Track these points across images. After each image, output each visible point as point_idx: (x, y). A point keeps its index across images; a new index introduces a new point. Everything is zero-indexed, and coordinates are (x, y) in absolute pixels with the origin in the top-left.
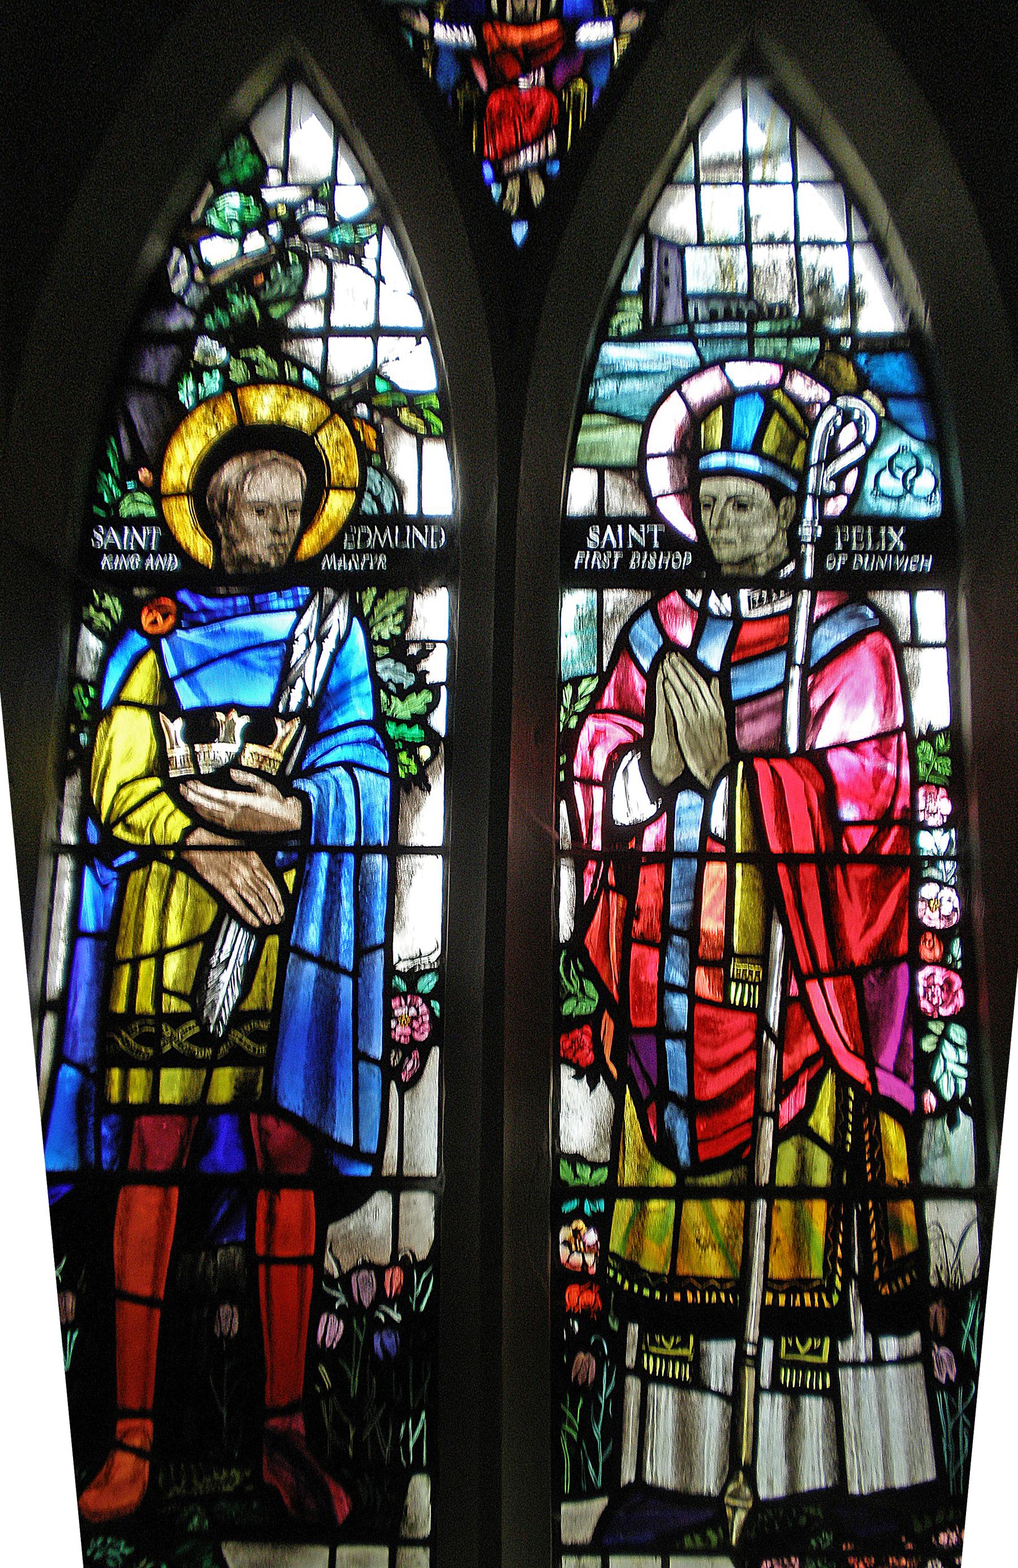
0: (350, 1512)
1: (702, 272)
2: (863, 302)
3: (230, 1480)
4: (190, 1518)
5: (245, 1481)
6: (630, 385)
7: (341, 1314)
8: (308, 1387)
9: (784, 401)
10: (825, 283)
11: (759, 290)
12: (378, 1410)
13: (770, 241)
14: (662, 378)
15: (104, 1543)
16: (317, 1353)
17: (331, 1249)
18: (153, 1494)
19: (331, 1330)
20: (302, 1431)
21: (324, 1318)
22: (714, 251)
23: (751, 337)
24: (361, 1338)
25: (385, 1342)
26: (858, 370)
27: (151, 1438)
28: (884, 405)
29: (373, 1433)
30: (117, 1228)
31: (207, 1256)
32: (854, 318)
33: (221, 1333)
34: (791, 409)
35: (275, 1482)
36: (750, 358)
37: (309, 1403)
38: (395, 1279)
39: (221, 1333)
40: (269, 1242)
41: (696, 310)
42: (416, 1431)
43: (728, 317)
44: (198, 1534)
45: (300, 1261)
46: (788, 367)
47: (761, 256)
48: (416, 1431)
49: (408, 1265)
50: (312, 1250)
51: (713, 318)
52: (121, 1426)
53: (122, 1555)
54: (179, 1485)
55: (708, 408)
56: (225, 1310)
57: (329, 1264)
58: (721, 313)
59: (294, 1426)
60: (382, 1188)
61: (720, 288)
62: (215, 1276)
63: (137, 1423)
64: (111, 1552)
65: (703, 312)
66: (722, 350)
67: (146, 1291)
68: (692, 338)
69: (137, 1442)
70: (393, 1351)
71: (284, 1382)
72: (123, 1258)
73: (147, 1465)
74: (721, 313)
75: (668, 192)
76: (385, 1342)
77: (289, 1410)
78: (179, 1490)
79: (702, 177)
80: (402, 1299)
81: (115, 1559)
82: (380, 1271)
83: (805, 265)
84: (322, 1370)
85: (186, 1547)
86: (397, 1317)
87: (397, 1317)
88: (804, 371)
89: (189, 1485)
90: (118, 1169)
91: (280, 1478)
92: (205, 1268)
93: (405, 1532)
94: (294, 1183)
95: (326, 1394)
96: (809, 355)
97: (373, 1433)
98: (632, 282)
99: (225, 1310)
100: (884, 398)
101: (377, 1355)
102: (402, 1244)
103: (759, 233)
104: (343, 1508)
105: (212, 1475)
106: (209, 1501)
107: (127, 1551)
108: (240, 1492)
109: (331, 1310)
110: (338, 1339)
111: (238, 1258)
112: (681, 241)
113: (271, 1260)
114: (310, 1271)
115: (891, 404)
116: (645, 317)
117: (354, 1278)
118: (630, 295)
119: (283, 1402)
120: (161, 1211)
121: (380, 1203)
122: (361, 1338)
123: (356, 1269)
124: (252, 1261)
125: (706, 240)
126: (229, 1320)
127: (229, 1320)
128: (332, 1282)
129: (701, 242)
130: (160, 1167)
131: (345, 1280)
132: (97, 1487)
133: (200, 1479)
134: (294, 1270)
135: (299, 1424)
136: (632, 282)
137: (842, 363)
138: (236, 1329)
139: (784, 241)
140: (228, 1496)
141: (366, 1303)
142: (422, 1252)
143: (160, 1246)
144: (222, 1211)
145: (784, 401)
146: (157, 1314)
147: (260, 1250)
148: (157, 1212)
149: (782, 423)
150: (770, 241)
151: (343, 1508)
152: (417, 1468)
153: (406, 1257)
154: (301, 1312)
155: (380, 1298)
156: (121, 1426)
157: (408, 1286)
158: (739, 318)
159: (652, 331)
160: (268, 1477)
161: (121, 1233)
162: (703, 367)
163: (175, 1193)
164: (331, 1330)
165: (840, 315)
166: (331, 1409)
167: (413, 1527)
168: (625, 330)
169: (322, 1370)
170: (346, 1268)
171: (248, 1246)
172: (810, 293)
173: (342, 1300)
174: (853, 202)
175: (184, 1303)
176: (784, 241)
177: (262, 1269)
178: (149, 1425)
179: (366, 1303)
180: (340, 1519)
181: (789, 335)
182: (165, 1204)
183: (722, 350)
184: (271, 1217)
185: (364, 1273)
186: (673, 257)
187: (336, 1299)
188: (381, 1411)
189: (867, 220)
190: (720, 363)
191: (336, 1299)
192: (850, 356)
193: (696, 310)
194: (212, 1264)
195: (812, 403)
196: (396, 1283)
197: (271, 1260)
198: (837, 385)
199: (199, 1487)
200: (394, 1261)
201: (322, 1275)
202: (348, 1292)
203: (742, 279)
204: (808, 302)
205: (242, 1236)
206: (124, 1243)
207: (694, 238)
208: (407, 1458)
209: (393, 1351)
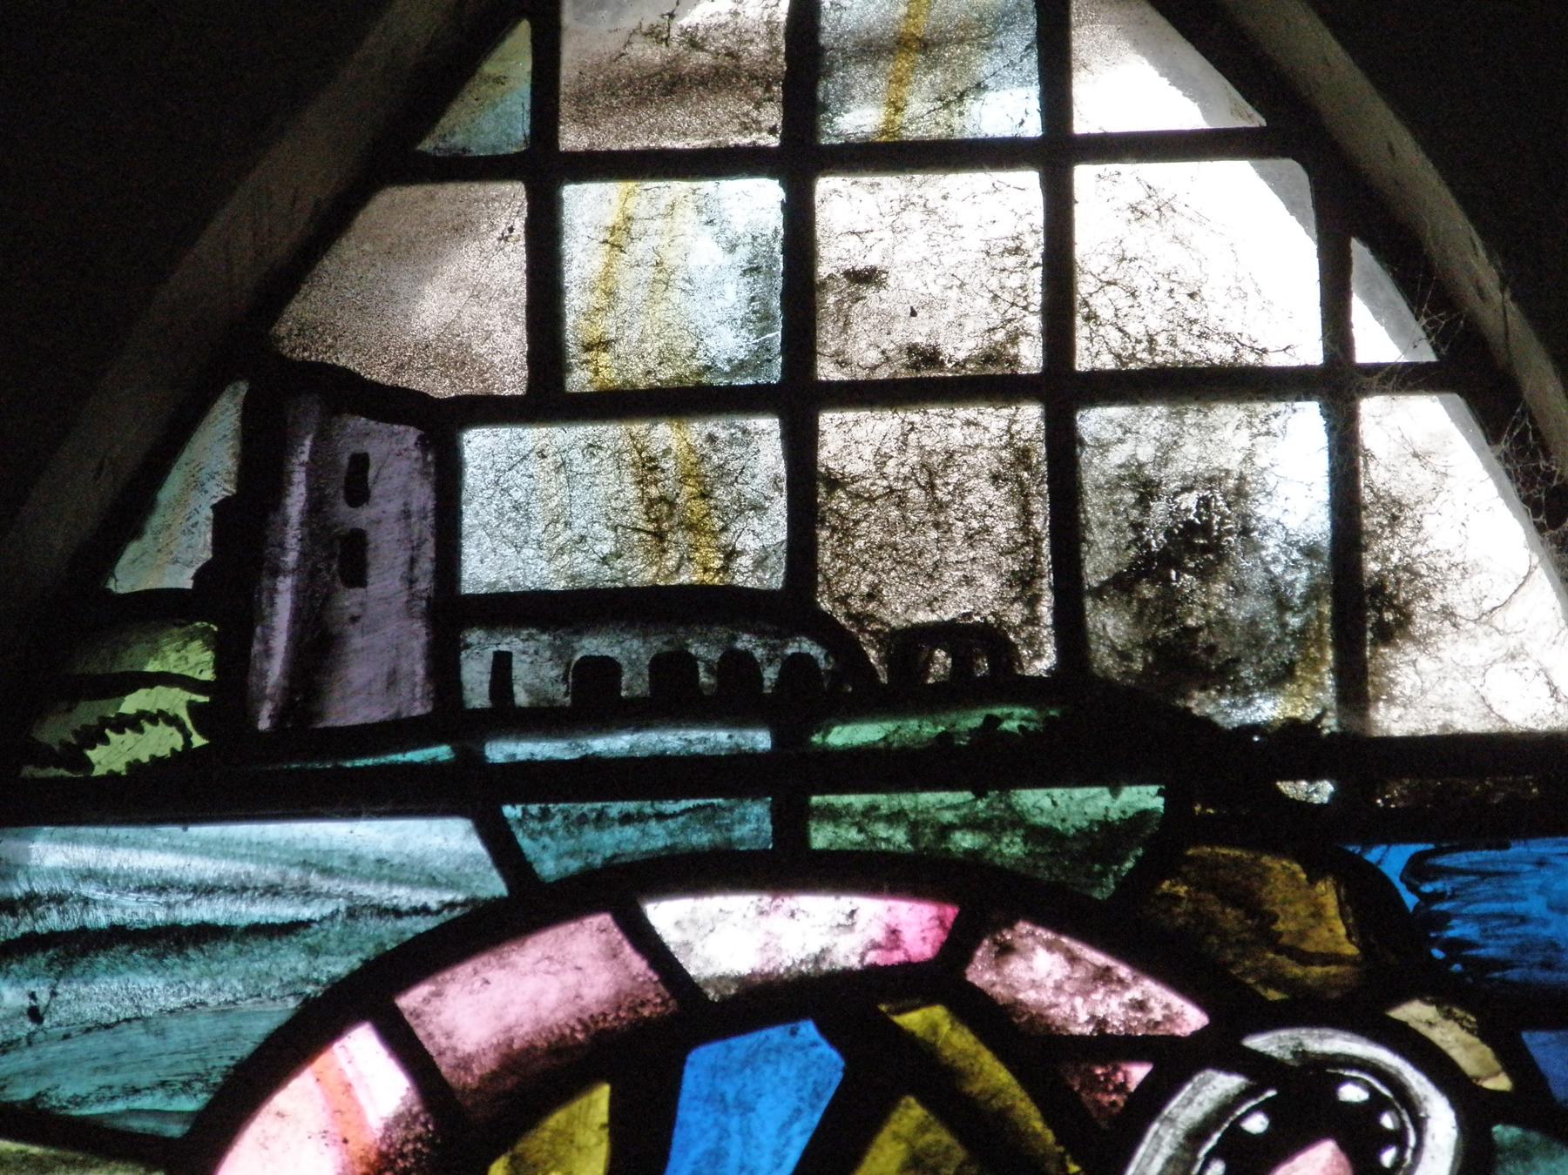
1: (539, 512)
2: (1405, 618)
6: (103, 992)
9: (957, 1041)
10: (1200, 544)
11: (845, 581)
13: (921, 383)
14: (291, 962)
22: (612, 433)
23: (793, 778)
26: (1367, 899)
28: (1512, 1057)
32: (1355, 687)
34: (993, 1075)
36: (786, 868)
41: (502, 663)
43: (673, 696)
46: (986, 901)
47: (851, 440)
51: (594, 698)
55: (539, 1076)
58: (634, 683)
61: (641, 572)
65: (536, 669)
66: (623, 834)
68: (467, 791)
74: (634, 683)
75: (396, 208)
79: (572, 138)
83: (1097, 468)
88: (1071, 917)
96: (1109, 837)
98: (170, 553)
100: (1503, 1013)
103: (857, 345)
112: (442, 388)
115: (1538, 1043)
116: (224, 704)
118: (162, 611)
125: (579, 380)
129: (547, 397)
136: (170, 553)
137: (1282, 872)
139: (990, 383)
145: (957, 1041)
149: (940, 1137)
150: (921, 383)
158: (735, 697)
159: (253, 764)
162: (523, 908)
165: (1280, 678)
168: (109, 757)
172: (1121, 584)
174: (1353, 218)
176: (990, 383)
181: (990, 765)
183: (623, 834)
186: (395, 455)
189: (1421, 284)
190: (618, 891)
192: (1320, 843)
193: (502, 663)
195: (1109, 1046)
198: (1246, 970)
203: (765, 532)
204: (1109, 625)
207: (512, 382)
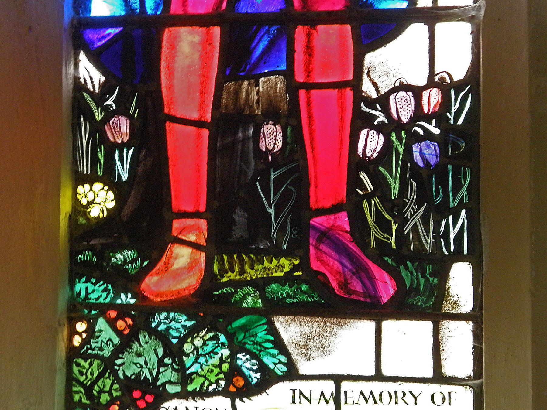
0: (396, 293)
3: (280, 267)
4: (244, 297)
5: (295, 268)
7: (380, 129)
8: (351, 191)
12: (418, 209)
15: (167, 318)
16: (358, 163)
17: (368, 74)
18: (210, 280)
19: (371, 143)
20: (348, 228)
21: (364, 133)
24: (401, 149)
25: (425, 153)
27: (206, 233)
29: (415, 226)
30: (163, 64)
31: (249, 84)
33: (266, 148)
35: (322, 269)
37: (353, 205)
38: (432, 99)
39: (266, 148)
40: (308, 72)
42: (456, 226)
44: (252, 311)
45: (340, 85)
48: (456, 226)
49: (446, 87)
50: (350, 77)
52: (176, 224)
53: (183, 326)
54: (233, 272)
56: (269, 128)
57: (367, 88)
59: (339, 223)
60: (418, 20)
62: (258, 102)
63: (191, 222)
64: (174, 324)
67: (194, 115)
69: (192, 238)
70: (433, 161)
71: (326, 185)
72: (170, 87)
73: (203, 254)
76: (425, 153)
77: (335, 209)
78: (232, 276)
80: (439, 115)
81: (177, 330)
82: (417, 92)
84: (363, 176)
85: (242, 321)
86: (436, 131)
87: (436, 131)
89: (242, 272)
90: (161, 14)
91: (328, 264)
92: (248, 94)
93: (447, 308)
94: (331, 18)
95: (368, 197)
97: (415, 226)
99: (269, 128)
101: (416, 164)
102: (438, 69)
104: (387, 289)
105: (263, 264)
106: (260, 285)
107: (189, 324)
108: (288, 279)
109: (371, 127)
110: (378, 149)
111: (279, 85)
113: (309, 86)
114: (349, 93)
117: (392, 97)
119: (327, 204)
120: (204, 48)
121: (417, 32)
122: (401, 149)
123: (395, 90)
124: (293, 88)
126: (272, 137)
127: (272, 137)
128: (371, 103)
130: (201, 11)
131: (383, 101)
132: (157, 274)
133: (252, 268)
134: (334, 92)
135: (343, 220)
138: (280, 144)
140: (277, 280)
141: (405, 120)
142: (459, 73)
143: (205, 77)
144: (262, 45)
146: (206, 133)
147: (300, 77)
148: (200, 48)
151: (387, 289)
152: (458, 256)
153: (442, 79)
154: (342, 129)
155: (419, 115)
156: (176, 224)
157: (445, 104)
160: (315, 265)
161: (168, 67)
163: (217, 31)
164: (371, 143)
166: (373, 209)
167: (455, 304)
169: (363, 176)
170: (383, 91)
171: (289, 74)
173: (382, 118)
175: (229, 125)
177: (302, 93)
178: (203, 223)
179: (405, 120)
180: (385, 300)
182: (207, 42)
184: (309, 50)
185: (402, 94)
187: (377, 117)
188: (423, 209)
191: (377, 117)
194: (255, 90)
196: (433, 102)
197: (309, 86)
199: (251, 274)
200: (431, 83)
201: (359, 97)
202: (386, 110)
205: (283, 67)
206: (171, 75)
208: (448, 247)
209: (433, 161)
